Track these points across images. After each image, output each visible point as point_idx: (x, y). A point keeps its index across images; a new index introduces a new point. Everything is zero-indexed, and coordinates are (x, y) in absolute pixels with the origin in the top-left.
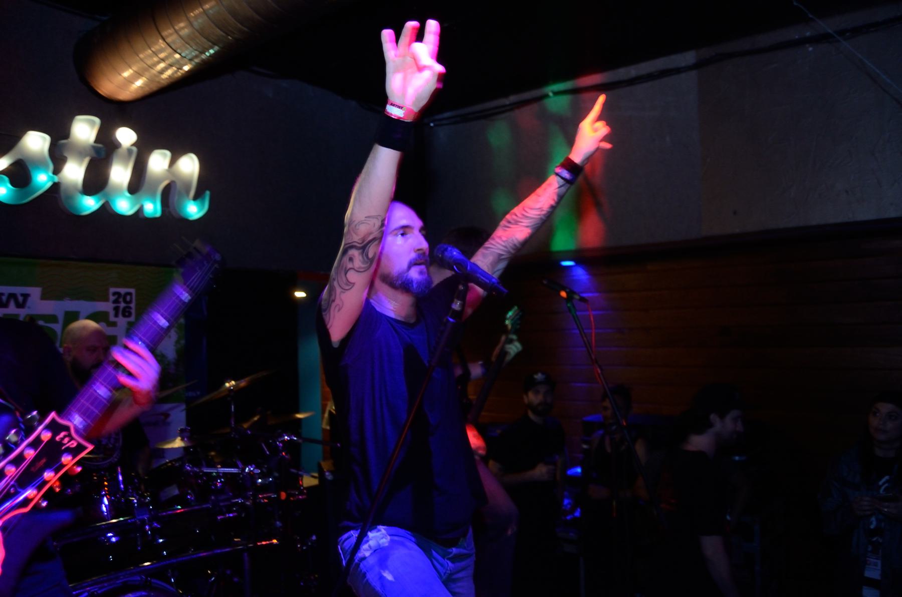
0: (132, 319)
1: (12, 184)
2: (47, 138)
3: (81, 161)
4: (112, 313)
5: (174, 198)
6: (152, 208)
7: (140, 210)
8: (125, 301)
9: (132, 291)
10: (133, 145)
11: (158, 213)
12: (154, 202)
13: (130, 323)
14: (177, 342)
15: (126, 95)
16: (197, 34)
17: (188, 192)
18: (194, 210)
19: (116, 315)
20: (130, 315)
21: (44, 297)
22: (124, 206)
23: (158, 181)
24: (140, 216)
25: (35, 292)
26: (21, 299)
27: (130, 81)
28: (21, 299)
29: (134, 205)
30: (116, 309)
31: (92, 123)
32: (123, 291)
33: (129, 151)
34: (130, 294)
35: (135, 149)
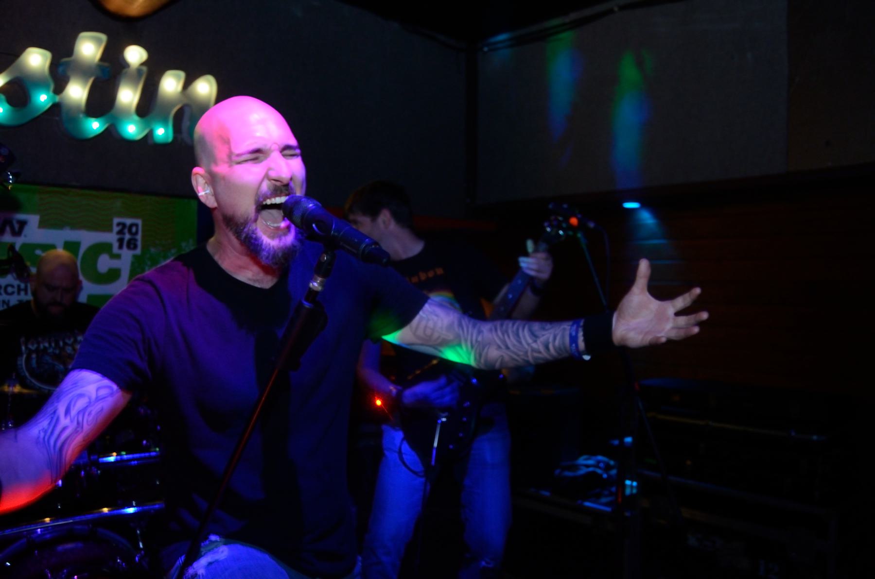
2: (48, 55)
3: (86, 81)
4: (116, 245)
5: (186, 124)
6: (162, 133)
7: (150, 135)
9: (139, 222)
10: (143, 64)
11: (170, 138)
19: (121, 247)
20: (135, 247)
21: (43, 224)
22: (132, 130)
23: (168, 105)
25: (33, 220)
26: (17, 226)
28: (17, 226)
29: (143, 131)
30: (121, 241)
31: (98, 41)
32: (128, 221)
33: (139, 71)
34: (137, 225)
35: (145, 69)
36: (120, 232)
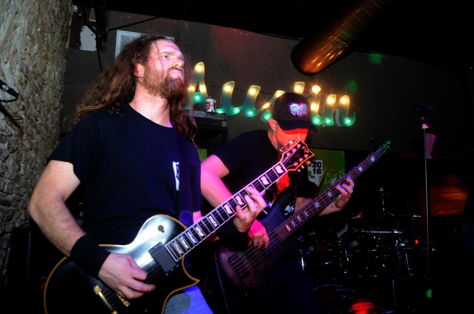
4: (313, 172)
6: (329, 121)
8: (318, 166)
9: (321, 161)
10: (320, 92)
11: (332, 124)
12: (330, 119)
13: (320, 177)
15: (315, 70)
18: (348, 122)
19: (314, 173)
20: (320, 173)
24: (324, 126)
27: (318, 62)
30: (314, 170)
31: (301, 85)
34: (320, 163)
35: (320, 95)
36: (313, 167)
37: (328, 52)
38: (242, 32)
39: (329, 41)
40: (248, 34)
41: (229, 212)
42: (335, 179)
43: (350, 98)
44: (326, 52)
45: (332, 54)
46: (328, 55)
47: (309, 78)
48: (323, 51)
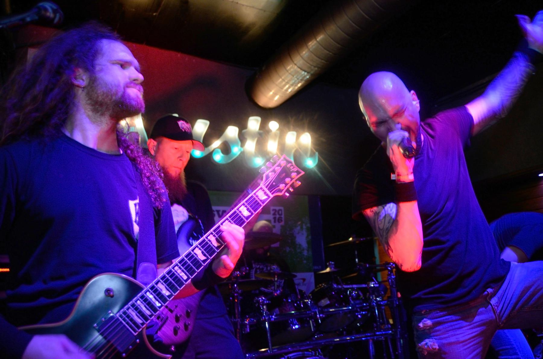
0: (282, 223)
1: (223, 152)
3: (253, 140)
8: (279, 214)
9: (282, 208)
13: (282, 226)
14: (307, 237)
16: (313, 55)
17: (306, 153)
18: (311, 163)
19: (275, 222)
20: (282, 221)
27: (275, 94)
30: (275, 218)
31: (257, 120)
32: (277, 208)
35: (278, 132)
36: (274, 214)
37: (287, 83)
38: (187, 58)
39: (288, 71)
40: (195, 60)
41: (201, 257)
42: (299, 228)
43: (311, 135)
44: (284, 83)
45: (292, 85)
46: (287, 86)
47: (266, 113)
48: (281, 82)
